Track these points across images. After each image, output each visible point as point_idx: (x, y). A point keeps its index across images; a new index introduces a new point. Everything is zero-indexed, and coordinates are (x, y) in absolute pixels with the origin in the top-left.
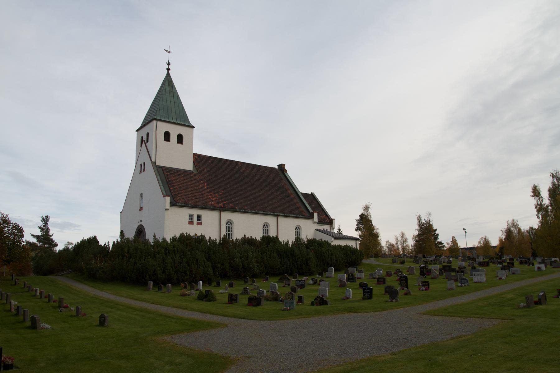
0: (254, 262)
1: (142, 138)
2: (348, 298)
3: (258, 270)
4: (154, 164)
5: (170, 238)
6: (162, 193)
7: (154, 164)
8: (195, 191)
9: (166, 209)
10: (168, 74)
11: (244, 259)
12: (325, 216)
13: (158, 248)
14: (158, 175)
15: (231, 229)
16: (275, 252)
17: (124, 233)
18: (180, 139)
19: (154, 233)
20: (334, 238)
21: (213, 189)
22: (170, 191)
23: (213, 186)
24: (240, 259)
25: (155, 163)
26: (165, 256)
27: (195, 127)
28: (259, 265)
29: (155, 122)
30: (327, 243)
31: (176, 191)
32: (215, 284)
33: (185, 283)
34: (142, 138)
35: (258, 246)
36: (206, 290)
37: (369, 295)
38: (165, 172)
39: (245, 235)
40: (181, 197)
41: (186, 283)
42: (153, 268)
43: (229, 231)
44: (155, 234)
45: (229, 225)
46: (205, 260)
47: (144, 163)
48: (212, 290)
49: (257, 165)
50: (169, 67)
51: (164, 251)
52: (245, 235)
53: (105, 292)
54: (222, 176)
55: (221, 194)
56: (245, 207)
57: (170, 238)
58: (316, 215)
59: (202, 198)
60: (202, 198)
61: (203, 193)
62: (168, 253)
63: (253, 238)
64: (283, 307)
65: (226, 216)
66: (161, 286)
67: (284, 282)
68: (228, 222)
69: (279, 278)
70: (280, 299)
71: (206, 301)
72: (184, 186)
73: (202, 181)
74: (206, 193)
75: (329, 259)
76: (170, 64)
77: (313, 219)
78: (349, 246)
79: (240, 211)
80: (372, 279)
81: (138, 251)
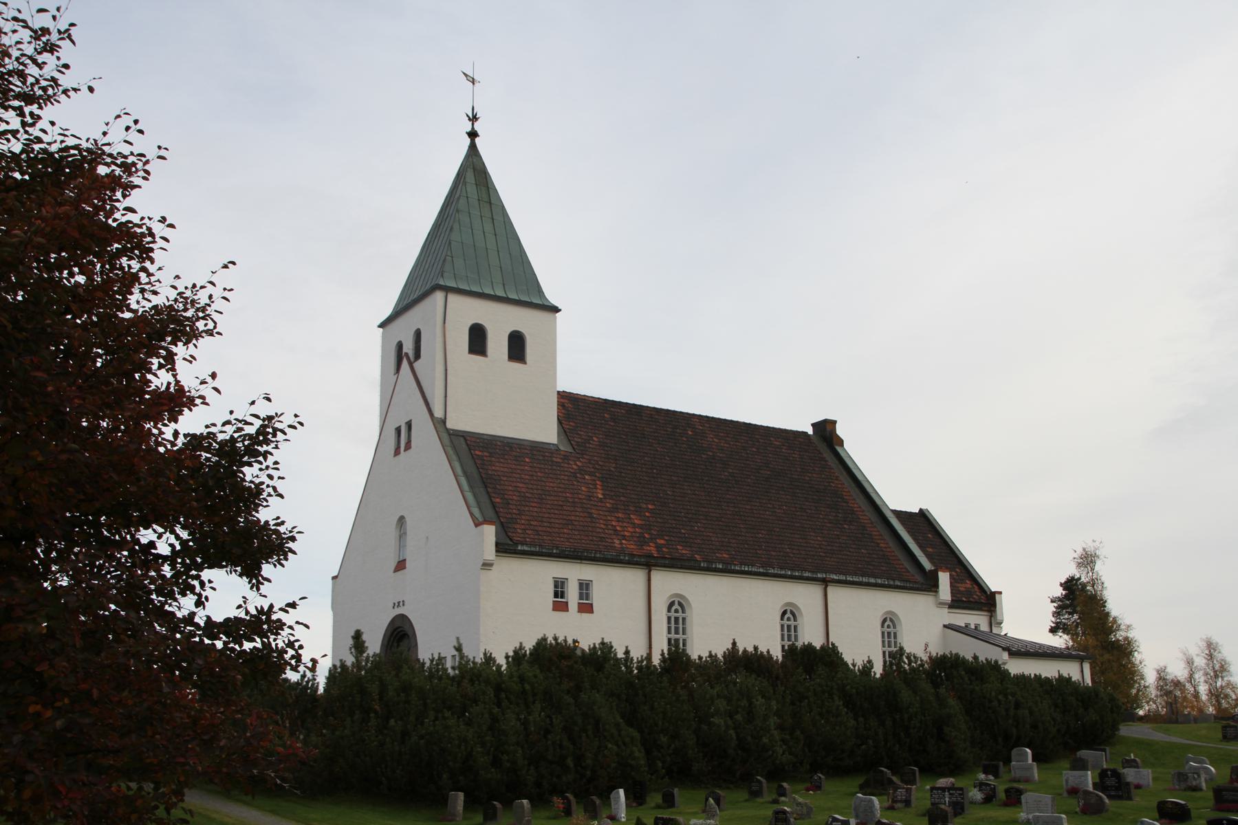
0: (773, 728)
1: (400, 346)
3: (787, 753)
4: (440, 424)
5: (507, 654)
6: (471, 514)
7: (440, 424)
8: (569, 508)
9: (484, 564)
10: (473, 148)
11: (741, 719)
12: (968, 582)
13: (473, 685)
14: (454, 457)
15: (683, 624)
16: (836, 698)
17: (364, 637)
18: (517, 347)
19: (458, 639)
20: (1009, 655)
21: (622, 498)
22: (494, 507)
23: (621, 490)
24: (728, 718)
25: (444, 421)
26: (496, 710)
27: (560, 310)
28: (788, 737)
29: (439, 296)
30: (995, 667)
31: (511, 506)
32: (657, 798)
33: (567, 798)
34: (400, 346)
35: (777, 678)
36: (656, 818)
38: (474, 450)
39: (734, 644)
40: (527, 527)
43: (677, 632)
44: (461, 642)
45: (676, 611)
46: (621, 721)
47: (409, 425)
48: (678, 818)
49: (750, 424)
50: (477, 126)
51: (492, 695)
52: (734, 644)
54: (646, 458)
55: (647, 514)
56: (725, 555)
57: (507, 654)
58: (944, 578)
59: (590, 529)
60: (590, 529)
61: (593, 511)
62: (506, 701)
63: (762, 653)
65: (668, 583)
68: (672, 604)
69: (860, 780)
72: (535, 491)
73: (587, 477)
74: (601, 513)
75: (1010, 721)
76: (477, 119)
77: (936, 592)
78: (1070, 678)
79: (710, 570)
81: (413, 695)
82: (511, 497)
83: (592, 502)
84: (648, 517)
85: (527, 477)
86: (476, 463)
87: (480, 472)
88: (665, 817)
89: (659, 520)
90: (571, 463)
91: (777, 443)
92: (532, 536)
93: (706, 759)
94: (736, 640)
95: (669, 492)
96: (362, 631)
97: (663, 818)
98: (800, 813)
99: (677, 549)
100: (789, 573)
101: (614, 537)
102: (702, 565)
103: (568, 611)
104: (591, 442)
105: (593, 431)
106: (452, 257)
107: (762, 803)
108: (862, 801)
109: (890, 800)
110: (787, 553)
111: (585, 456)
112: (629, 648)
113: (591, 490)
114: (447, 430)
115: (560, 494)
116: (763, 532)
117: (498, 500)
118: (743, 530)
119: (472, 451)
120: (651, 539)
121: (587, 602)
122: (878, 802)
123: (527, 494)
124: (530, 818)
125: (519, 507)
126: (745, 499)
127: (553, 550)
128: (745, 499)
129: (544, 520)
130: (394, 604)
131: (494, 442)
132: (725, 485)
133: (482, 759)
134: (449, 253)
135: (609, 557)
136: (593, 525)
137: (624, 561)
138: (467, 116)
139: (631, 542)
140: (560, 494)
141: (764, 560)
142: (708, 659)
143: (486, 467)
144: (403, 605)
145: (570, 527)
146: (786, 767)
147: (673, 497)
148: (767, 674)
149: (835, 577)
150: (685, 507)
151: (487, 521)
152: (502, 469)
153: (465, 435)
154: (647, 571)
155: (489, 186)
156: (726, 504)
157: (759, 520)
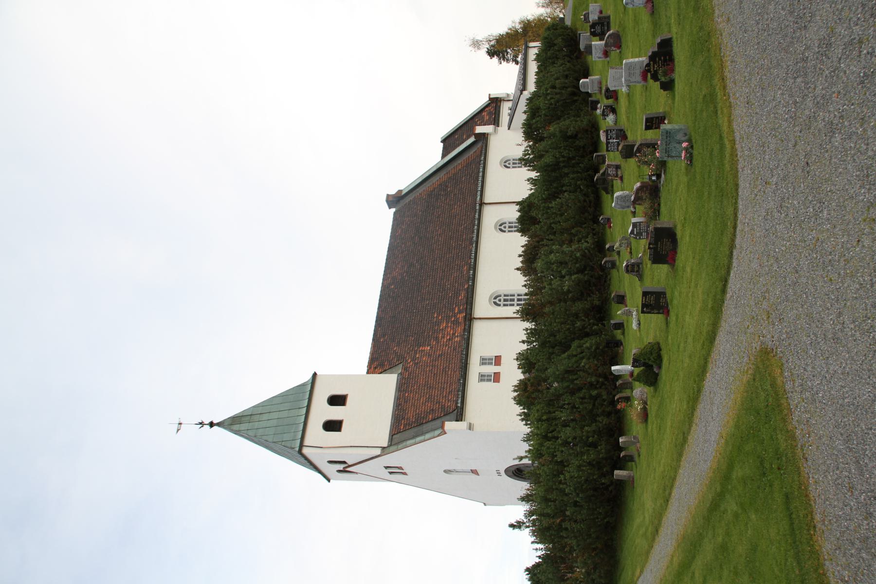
1: (339, 471)
3: (586, 240)
5: (524, 425)
6: (439, 435)
9: (470, 429)
10: (219, 424)
11: (565, 270)
12: (483, 114)
14: (404, 444)
15: (508, 296)
16: (550, 205)
18: (337, 400)
19: (514, 459)
20: (525, 90)
21: (430, 334)
22: (435, 419)
23: (426, 334)
24: (564, 279)
25: (383, 448)
26: (560, 441)
27: (315, 372)
28: (576, 238)
29: (305, 451)
30: (530, 100)
32: (618, 332)
34: (339, 471)
35: (538, 242)
39: (518, 269)
41: (616, 398)
42: (584, 468)
43: (513, 300)
44: (516, 457)
45: (500, 300)
46: (566, 354)
47: (386, 467)
48: (633, 354)
49: (388, 248)
51: (550, 443)
52: (518, 269)
53: (637, 580)
55: (440, 318)
57: (524, 425)
58: (479, 129)
59: (448, 356)
61: (438, 354)
62: (553, 433)
63: (523, 252)
64: (682, 163)
65: (482, 306)
67: (612, 181)
68: (495, 303)
70: (654, 178)
71: (660, 367)
73: (417, 356)
74: (439, 348)
75: (563, 92)
77: (488, 134)
79: (474, 279)
81: (550, 497)
82: (429, 408)
83: (433, 353)
84: (442, 317)
88: (632, 362)
89: (443, 310)
91: (400, 231)
93: (591, 295)
94: (516, 268)
95: (427, 302)
97: (633, 363)
98: (626, 244)
99: (461, 299)
100: (476, 227)
103: (499, 373)
107: (620, 261)
108: (617, 203)
110: (464, 227)
111: (405, 356)
112: (521, 341)
113: (425, 354)
114: (389, 446)
115: (427, 375)
116: (451, 243)
118: (450, 255)
121: (494, 360)
122: (618, 193)
123: (427, 397)
125: (435, 403)
126: (432, 253)
127: (460, 383)
128: (432, 253)
129: (443, 386)
131: (396, 416)
132: (423, 266)
133: (592, 456)
134: (280, 443)
140: (427, 375)
143: (411, 423)
145: (447, 370)
146: (596, 240)
147: (430, 300)
149: (479, 198)
150: (436, 292)
151: (442, 427)
152: (412, 412)
153: (391, 435)
154: (474, 320)
155: (241, 415)
156: (435, 266)
157: (444, 245)
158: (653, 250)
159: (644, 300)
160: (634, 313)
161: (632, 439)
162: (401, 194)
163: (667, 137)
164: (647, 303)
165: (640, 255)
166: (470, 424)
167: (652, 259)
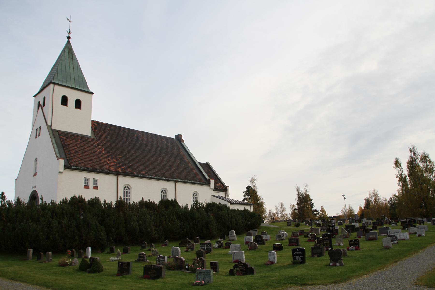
0: (152, 226)
1: (39, 102)
2: (272, 263)
3: (157, 234)
5: (61, 201)
6: (57, 156)
8: (92, 156)
9: (59, 172)
10: (69, 42)
12: (220, 183)
14: (53, 138)
15: (129, 194)
16: (174, 216)
18: (78, 104)
20: (230, 204)
21: (111, 154)
23: (111, 151)
24: (137, 222)
25: (51, 126)
26: (51, 220)
28: (158, 229)
29: (52, 86)
30: (226, 206)
31: (71, 154)
33: (73, 250)
34: (39, 102)
37: (301, 257)
38: (61, 136)
39: (143, 199)
40: (76, 161)
41: (73, 249)
42: (35, 233)
43: (127, 196)
44: (43, 196)
45: (127, 190)
46: (98, 223)
47: (40, 128)
48: (97, 258)
49: (155, 134)
50: (70, 35)
52: (143, 199)
54: (121, 142)
55: (119, 159)
56: (144, 172)
57: (61, 201)
58: (212, 181)
59: (99, 162)
60: (99, 162)
61: (100, 157)
63: (151, 202)
64: (194, 281)
65: (124, 181)
66: (41, 254)
67: (186, 246)
68: (125, 187)
71: (90, 272)
72: (81, 150)
73: (100, 147)
75: (229, 222)
76: (70, 33)
77: (210, 185)
79: (138, 177)
80: (280, 240)
82: (72, 151)
83: (101, 154)
84: (119, 160)
85: (79, 145)
86: (61, 140)
87: (62, 143)
89: (123, 161)
90: (95, 142)
92: (78, 164)
94: (143, 198)
96: (4, 192)
98: (154, 254)
99: (128, 170)
100: (164, 178)
101: (107, 165)
102: (136, 175)
104: (102, 136)
105: (104, 133)
106: (57, 74)
107: (145, 251)
109: (187, 248)
110: (164, 172)
111: (100, 140)
113: (100, 151)
114: (52, 130)
115: (89, 151)
116: (157, 166)
117: (67, 152)
118: (150, 165)
119: (60, 137)
120: (119, 166)
122: (180, 249)
124: (51, 258)
125: (74, 155)
126: (152, 156)
127: (84, 168)
128: (152, 156)
129: (83, 159)
130: (33, 187)
131: (68, 134)
132: (146, 151)
133: (42, 237)
134: (57, 73)
135: (104, 171)
136: (100, 161)
137: (109, 173)
138: (67, 32)
139: (113, 167)
140: (89, 151)
141: (156, 174)
142: (133, 204)
143: (64, 141)
144: (35, 187)
145: (92, 162)
146: (156, 239)
147: (128, 154)
148: (153, 209)
151: (61, 158)
156: (145, 157)
158: (151, 267)
159: (125, 263)
160: (118, 258)
161: (50, 259)
162: (182, 142)
163: (207, 273)
164: (123, 264)
165: (148, 261)
166: (62, 173)
167: (146, 267)
